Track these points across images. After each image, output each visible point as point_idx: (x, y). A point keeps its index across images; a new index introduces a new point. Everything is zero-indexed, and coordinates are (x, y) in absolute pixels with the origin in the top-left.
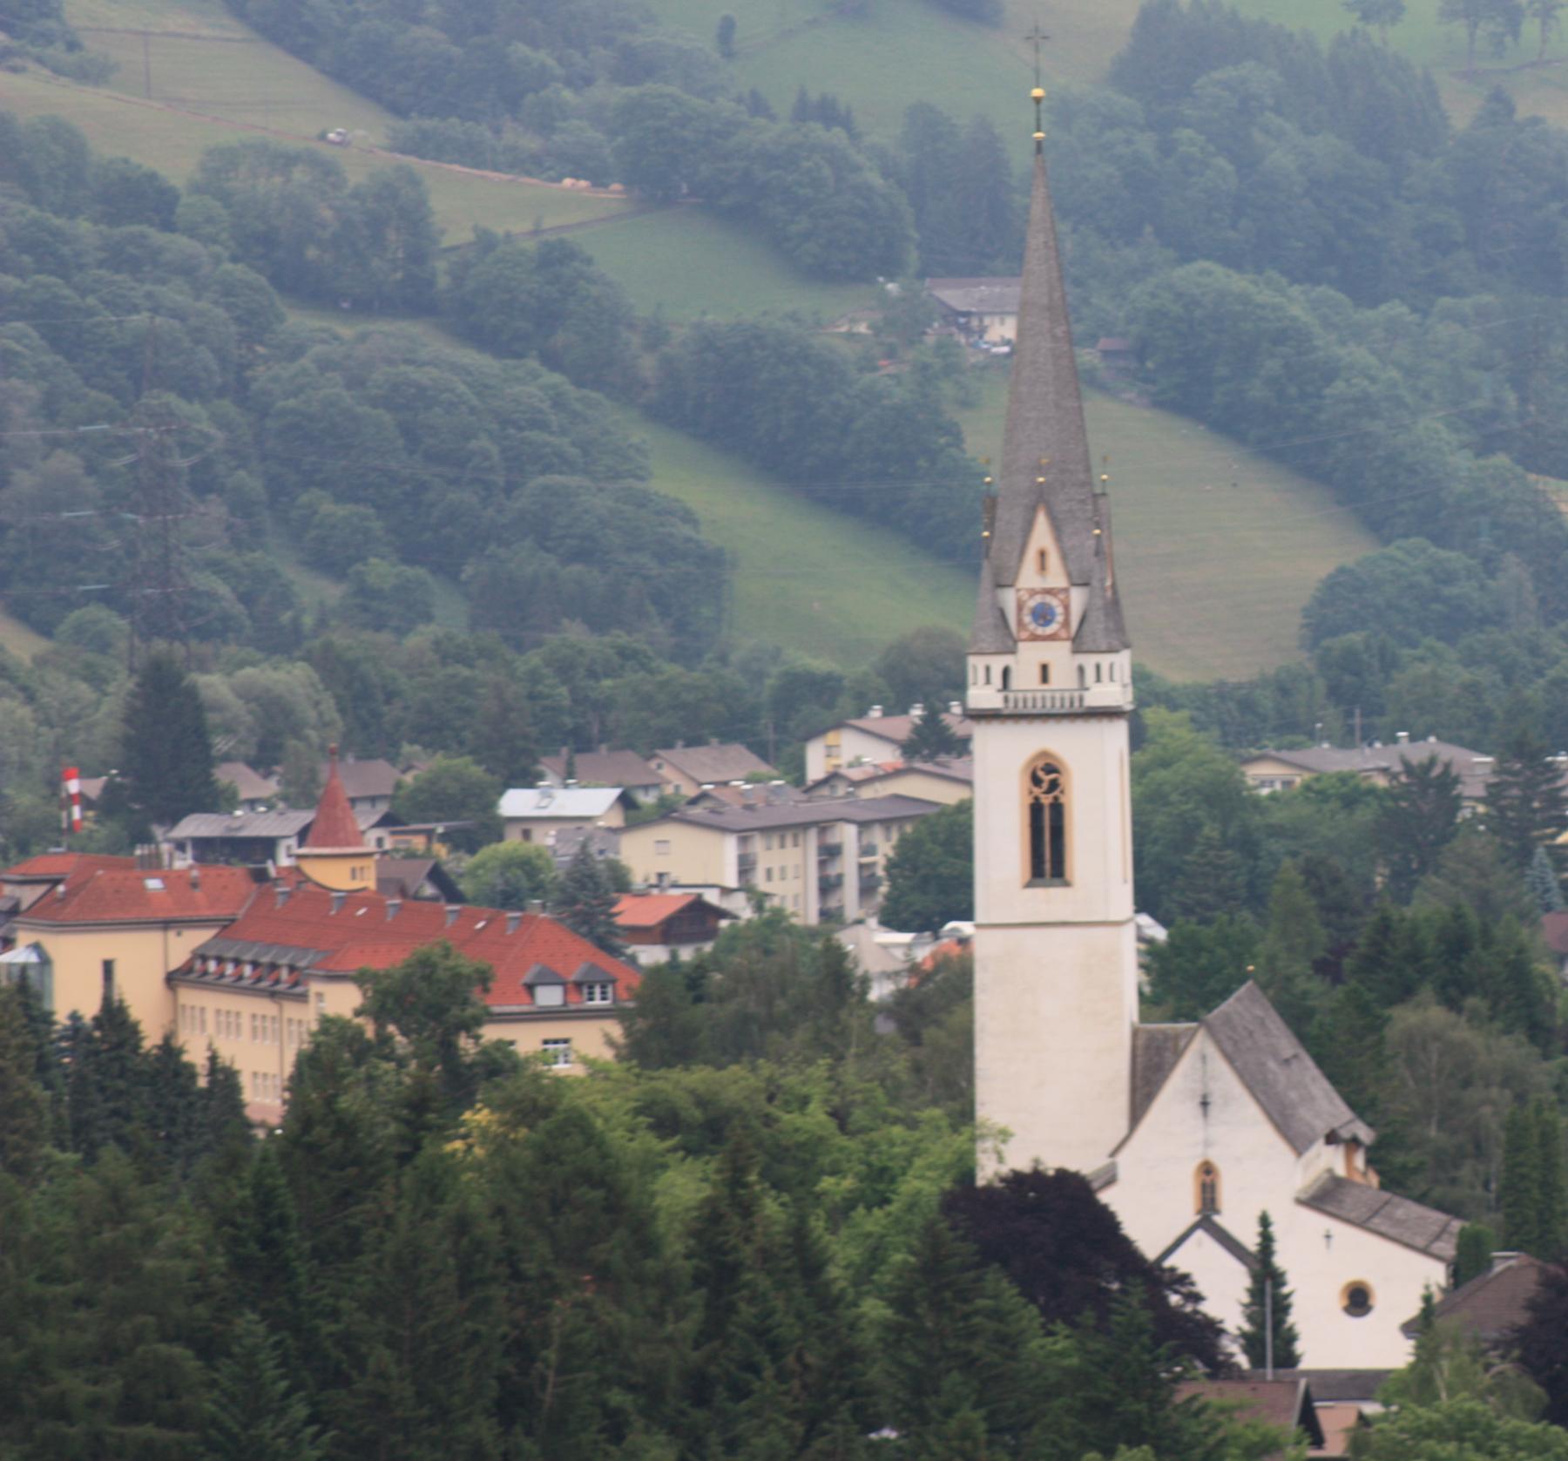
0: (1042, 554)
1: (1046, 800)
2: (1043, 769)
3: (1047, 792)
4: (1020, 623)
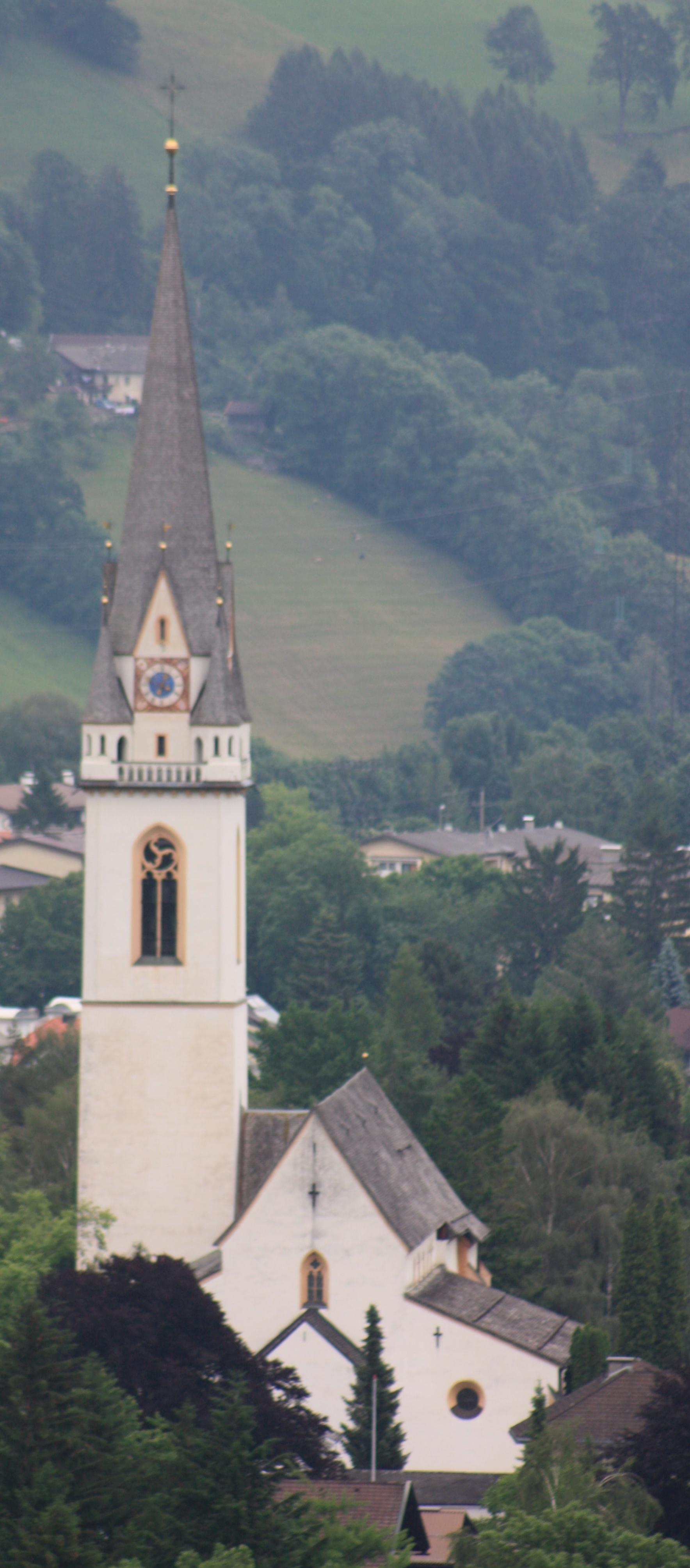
0: (162, 623)
1: (159, 876)
2: (156, 844)
4: (137, 692)
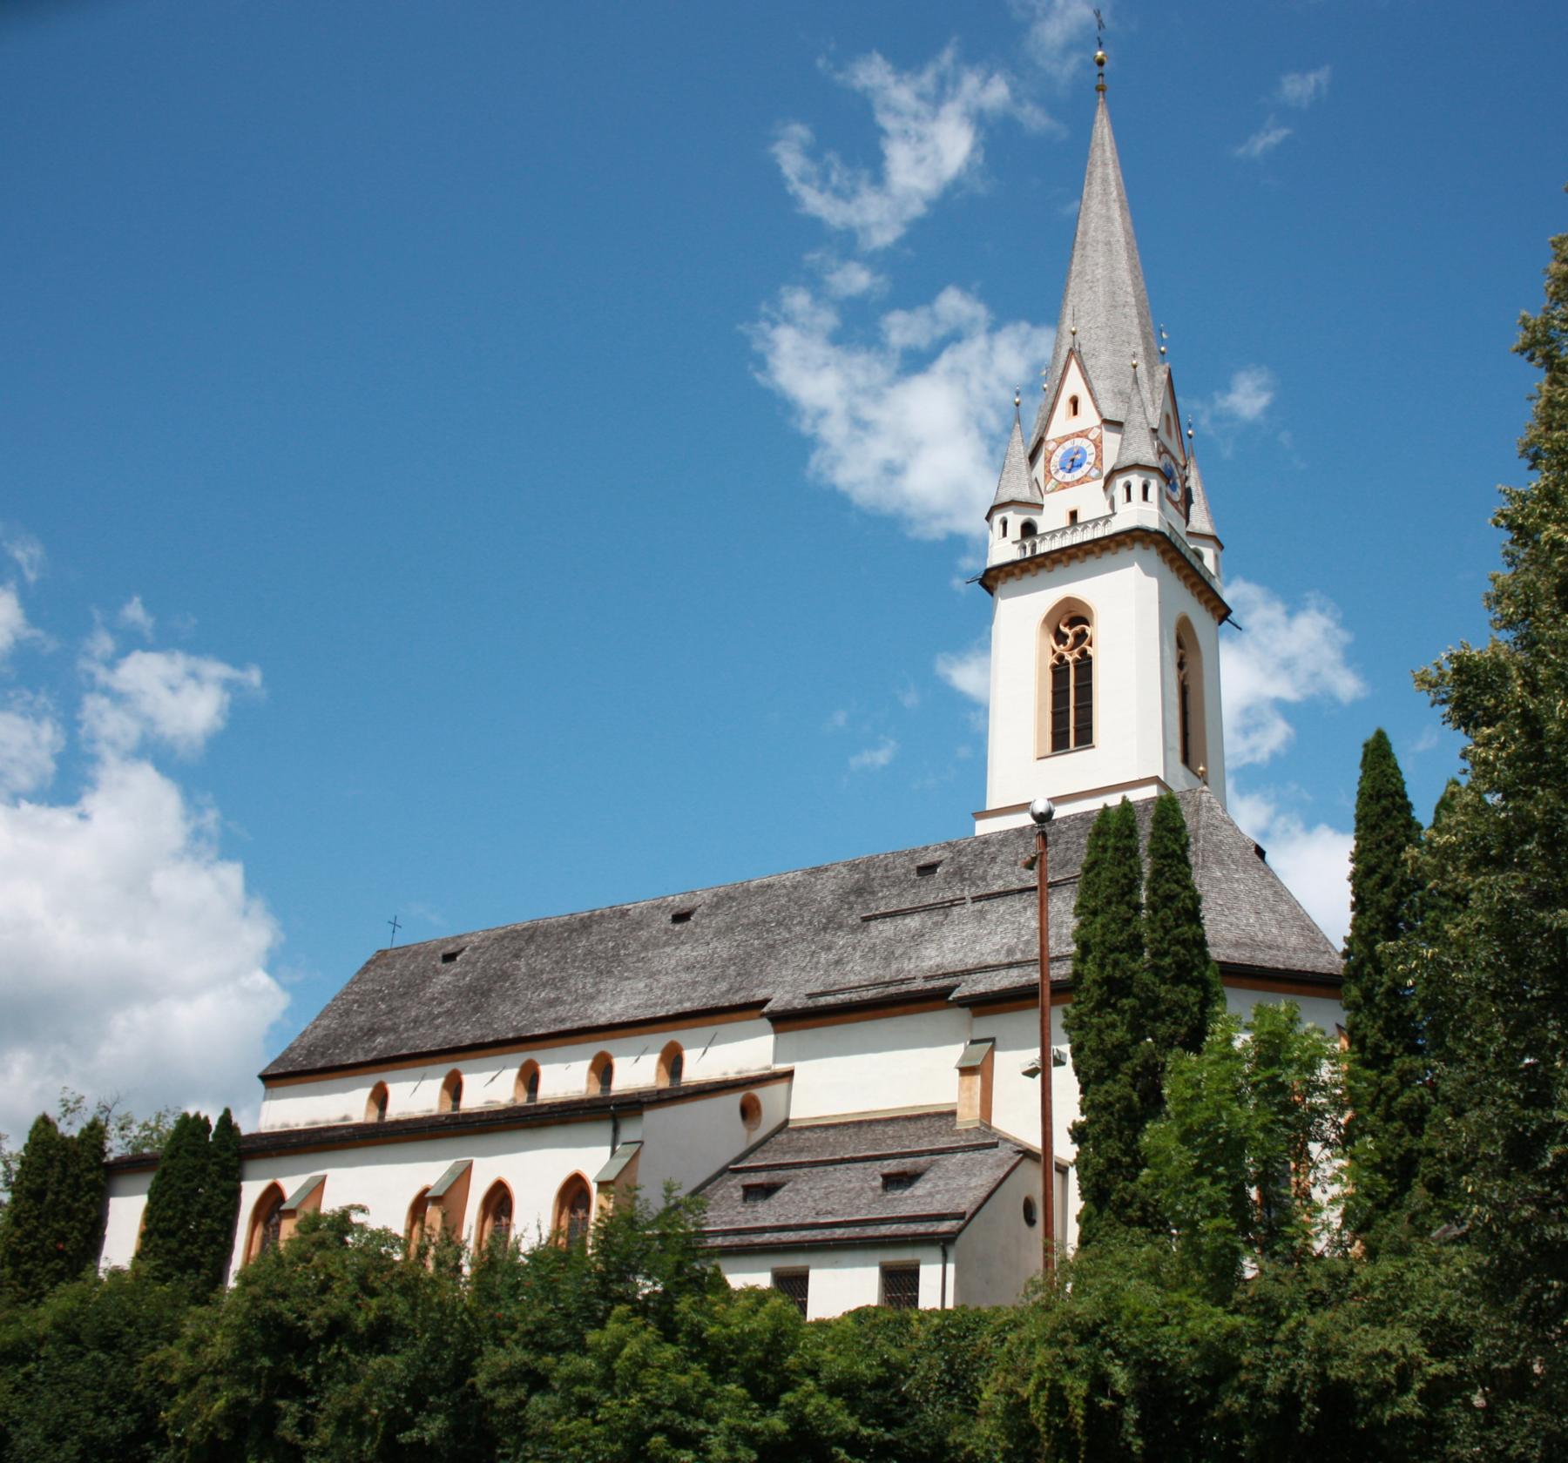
0: (1075, 402)
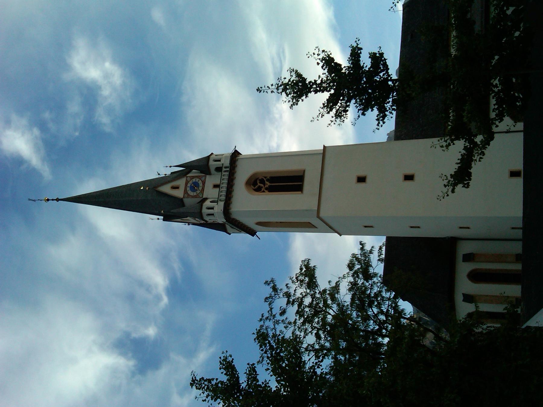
1: (268, 184)
2: (255, 187)
3: (264, 184)
